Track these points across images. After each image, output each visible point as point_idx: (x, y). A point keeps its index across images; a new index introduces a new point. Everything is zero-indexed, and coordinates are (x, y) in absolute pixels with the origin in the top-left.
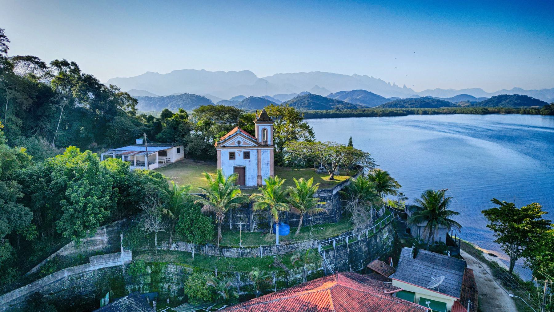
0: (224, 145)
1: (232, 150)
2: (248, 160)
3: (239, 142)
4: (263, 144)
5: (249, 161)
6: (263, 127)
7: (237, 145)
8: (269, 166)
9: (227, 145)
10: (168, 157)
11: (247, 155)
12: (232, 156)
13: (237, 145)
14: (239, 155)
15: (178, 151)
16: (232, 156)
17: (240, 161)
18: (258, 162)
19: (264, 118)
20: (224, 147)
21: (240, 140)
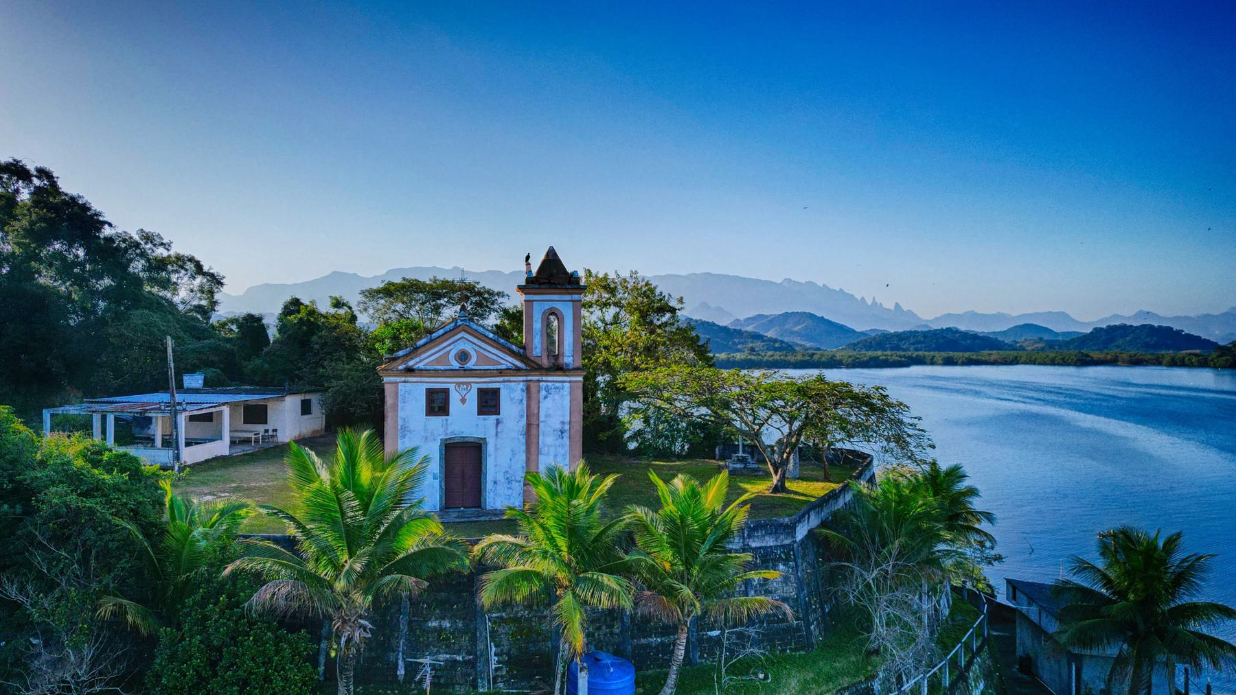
0: (411, 363)
1: (438, 383)
2: (492, 419)
3: (463, 356)
4: (545, 362)
5: (498, 422)
6: (547, 306)
7: (456, 365)
8: (566, 441)
9: (421, 366)
10: (270, 426)
11: (489, 402)
12: (437, 404)
13: (456, 365)
14: (463, 401)
15: (306, 408)
16: (437, 404)
17: (463, 419)
18: (529, 425)
19: (551, 275)
20: (410, 371)
21: (468, 348)
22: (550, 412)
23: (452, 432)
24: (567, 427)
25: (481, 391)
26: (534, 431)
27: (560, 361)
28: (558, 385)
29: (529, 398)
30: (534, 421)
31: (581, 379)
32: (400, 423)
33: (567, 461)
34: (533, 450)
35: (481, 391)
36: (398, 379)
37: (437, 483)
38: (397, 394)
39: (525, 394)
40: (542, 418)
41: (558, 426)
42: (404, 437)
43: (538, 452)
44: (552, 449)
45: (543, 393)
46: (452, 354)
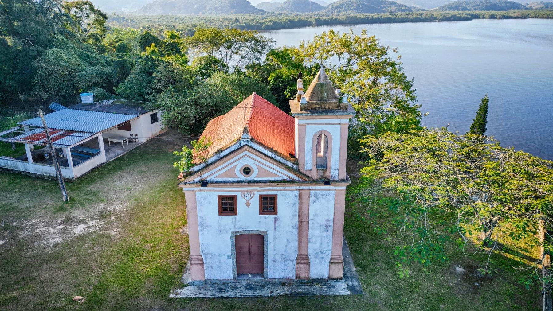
0: (204, 176)
1: (227, 191)
2: (271, 217)
3: (247, 171)
4: (315, 175)
5: (276, 220)
6: (319, 128)
7: (242, 177)
8: (330, 233)
9: (213, 178)
10: (133, 132)
11: (268, 205)
12: (227, 206)
13: (242, 177)
14: (248, 204)
15: (154, 119)
16: (227, 206)
17: (249, 218)
18: (300, 222)
19: (322, 100)
20: (204, 183)
21: (250, 163)
22: (318, 212)
23: (240, 227)
24: (331, 223)
25: (260, 196)
26: (304, 226)
27: (327, 174)
28: (324, 192)
29: (301, 202)
30: (304, 219)
31: (345, 187)
32: (199, 220)
33: (330, 247)
34: (304, 239)
35: (260, 196)
36: (195, 189)
37: (230, 261)
38: (195, 199)
39: (297, 200)
40: (311, 217)
41: (325, 223)
42: (203, 230)
43: (308, 241)
44: (318, 239)
45: (312, 199)
46: (238, 169)
